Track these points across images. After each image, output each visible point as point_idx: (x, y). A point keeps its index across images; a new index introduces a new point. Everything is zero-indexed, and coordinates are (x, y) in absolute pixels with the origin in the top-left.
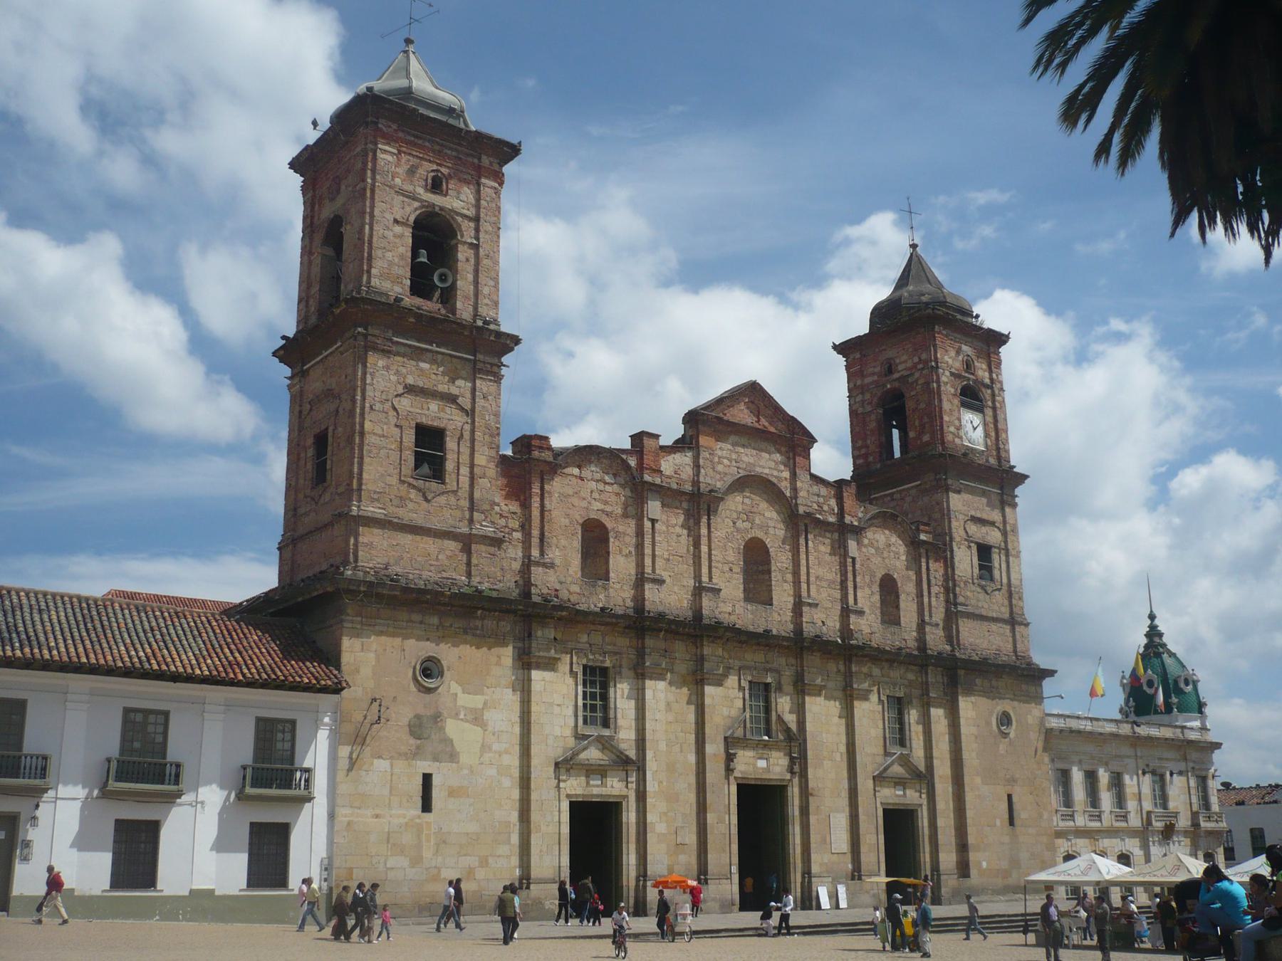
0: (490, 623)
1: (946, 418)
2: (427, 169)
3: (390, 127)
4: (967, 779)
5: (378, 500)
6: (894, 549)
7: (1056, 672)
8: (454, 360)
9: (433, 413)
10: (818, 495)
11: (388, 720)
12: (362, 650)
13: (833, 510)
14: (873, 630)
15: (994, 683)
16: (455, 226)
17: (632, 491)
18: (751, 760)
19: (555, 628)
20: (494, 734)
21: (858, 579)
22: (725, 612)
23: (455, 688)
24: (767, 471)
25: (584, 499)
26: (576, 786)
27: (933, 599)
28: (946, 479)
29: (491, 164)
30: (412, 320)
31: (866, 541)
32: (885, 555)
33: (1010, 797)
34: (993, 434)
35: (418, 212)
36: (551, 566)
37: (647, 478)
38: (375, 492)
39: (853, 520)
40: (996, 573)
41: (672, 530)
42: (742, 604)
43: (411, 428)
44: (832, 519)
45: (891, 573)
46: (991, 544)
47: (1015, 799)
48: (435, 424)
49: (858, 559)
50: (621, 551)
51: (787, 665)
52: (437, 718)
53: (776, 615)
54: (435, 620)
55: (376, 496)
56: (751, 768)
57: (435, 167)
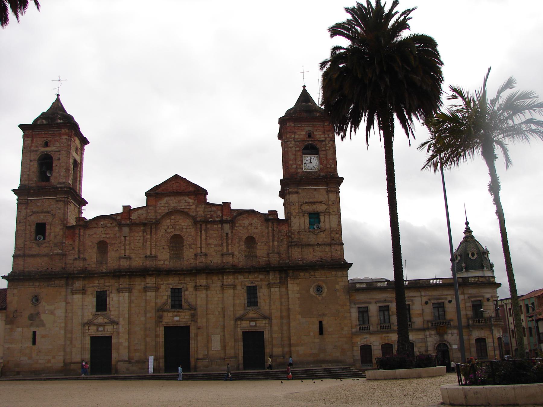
0: (57, 282)
1: (291, 162)
2: (40, 141)
4: (291, 317)
5: (21, 250)
6: (255, 225)
7: (352, 264)
8: (50, 200)
9: (41, 218)
10: (211, 211)
13: (219, 215)
14: (239, 260)
15: (312, 273)
16: (52, 156)
17: (118, 228)
18: (171, 318)
19: (83, 281)
20: (58, 317)
21: (230, 241)
22: (160, 265)
23: (44, 304)
24: (182, 208)
26: (92, 331)
27: (276, 243)
28: (289, 189)
29: (65, 131)
30: (32, 191)
31: (237, 225)
32: (249, 228)
33: (321, 323)
34: (325, 162)
36: (84, 259)
37: (123, 222)
39: (227, 217)
40: (322, 225)
42: (169, 260)
44: (217, 219)
45: (252, 235)
46: (319, 211)
47: (324, 323)
49: (230, 233)
50: (113, 250)
51: (191, 280)
52: (38, 314)
53: (185, 262)
54: (38, 284)
55: (21, 249)
56: (171, 321)
57: (45, 139)
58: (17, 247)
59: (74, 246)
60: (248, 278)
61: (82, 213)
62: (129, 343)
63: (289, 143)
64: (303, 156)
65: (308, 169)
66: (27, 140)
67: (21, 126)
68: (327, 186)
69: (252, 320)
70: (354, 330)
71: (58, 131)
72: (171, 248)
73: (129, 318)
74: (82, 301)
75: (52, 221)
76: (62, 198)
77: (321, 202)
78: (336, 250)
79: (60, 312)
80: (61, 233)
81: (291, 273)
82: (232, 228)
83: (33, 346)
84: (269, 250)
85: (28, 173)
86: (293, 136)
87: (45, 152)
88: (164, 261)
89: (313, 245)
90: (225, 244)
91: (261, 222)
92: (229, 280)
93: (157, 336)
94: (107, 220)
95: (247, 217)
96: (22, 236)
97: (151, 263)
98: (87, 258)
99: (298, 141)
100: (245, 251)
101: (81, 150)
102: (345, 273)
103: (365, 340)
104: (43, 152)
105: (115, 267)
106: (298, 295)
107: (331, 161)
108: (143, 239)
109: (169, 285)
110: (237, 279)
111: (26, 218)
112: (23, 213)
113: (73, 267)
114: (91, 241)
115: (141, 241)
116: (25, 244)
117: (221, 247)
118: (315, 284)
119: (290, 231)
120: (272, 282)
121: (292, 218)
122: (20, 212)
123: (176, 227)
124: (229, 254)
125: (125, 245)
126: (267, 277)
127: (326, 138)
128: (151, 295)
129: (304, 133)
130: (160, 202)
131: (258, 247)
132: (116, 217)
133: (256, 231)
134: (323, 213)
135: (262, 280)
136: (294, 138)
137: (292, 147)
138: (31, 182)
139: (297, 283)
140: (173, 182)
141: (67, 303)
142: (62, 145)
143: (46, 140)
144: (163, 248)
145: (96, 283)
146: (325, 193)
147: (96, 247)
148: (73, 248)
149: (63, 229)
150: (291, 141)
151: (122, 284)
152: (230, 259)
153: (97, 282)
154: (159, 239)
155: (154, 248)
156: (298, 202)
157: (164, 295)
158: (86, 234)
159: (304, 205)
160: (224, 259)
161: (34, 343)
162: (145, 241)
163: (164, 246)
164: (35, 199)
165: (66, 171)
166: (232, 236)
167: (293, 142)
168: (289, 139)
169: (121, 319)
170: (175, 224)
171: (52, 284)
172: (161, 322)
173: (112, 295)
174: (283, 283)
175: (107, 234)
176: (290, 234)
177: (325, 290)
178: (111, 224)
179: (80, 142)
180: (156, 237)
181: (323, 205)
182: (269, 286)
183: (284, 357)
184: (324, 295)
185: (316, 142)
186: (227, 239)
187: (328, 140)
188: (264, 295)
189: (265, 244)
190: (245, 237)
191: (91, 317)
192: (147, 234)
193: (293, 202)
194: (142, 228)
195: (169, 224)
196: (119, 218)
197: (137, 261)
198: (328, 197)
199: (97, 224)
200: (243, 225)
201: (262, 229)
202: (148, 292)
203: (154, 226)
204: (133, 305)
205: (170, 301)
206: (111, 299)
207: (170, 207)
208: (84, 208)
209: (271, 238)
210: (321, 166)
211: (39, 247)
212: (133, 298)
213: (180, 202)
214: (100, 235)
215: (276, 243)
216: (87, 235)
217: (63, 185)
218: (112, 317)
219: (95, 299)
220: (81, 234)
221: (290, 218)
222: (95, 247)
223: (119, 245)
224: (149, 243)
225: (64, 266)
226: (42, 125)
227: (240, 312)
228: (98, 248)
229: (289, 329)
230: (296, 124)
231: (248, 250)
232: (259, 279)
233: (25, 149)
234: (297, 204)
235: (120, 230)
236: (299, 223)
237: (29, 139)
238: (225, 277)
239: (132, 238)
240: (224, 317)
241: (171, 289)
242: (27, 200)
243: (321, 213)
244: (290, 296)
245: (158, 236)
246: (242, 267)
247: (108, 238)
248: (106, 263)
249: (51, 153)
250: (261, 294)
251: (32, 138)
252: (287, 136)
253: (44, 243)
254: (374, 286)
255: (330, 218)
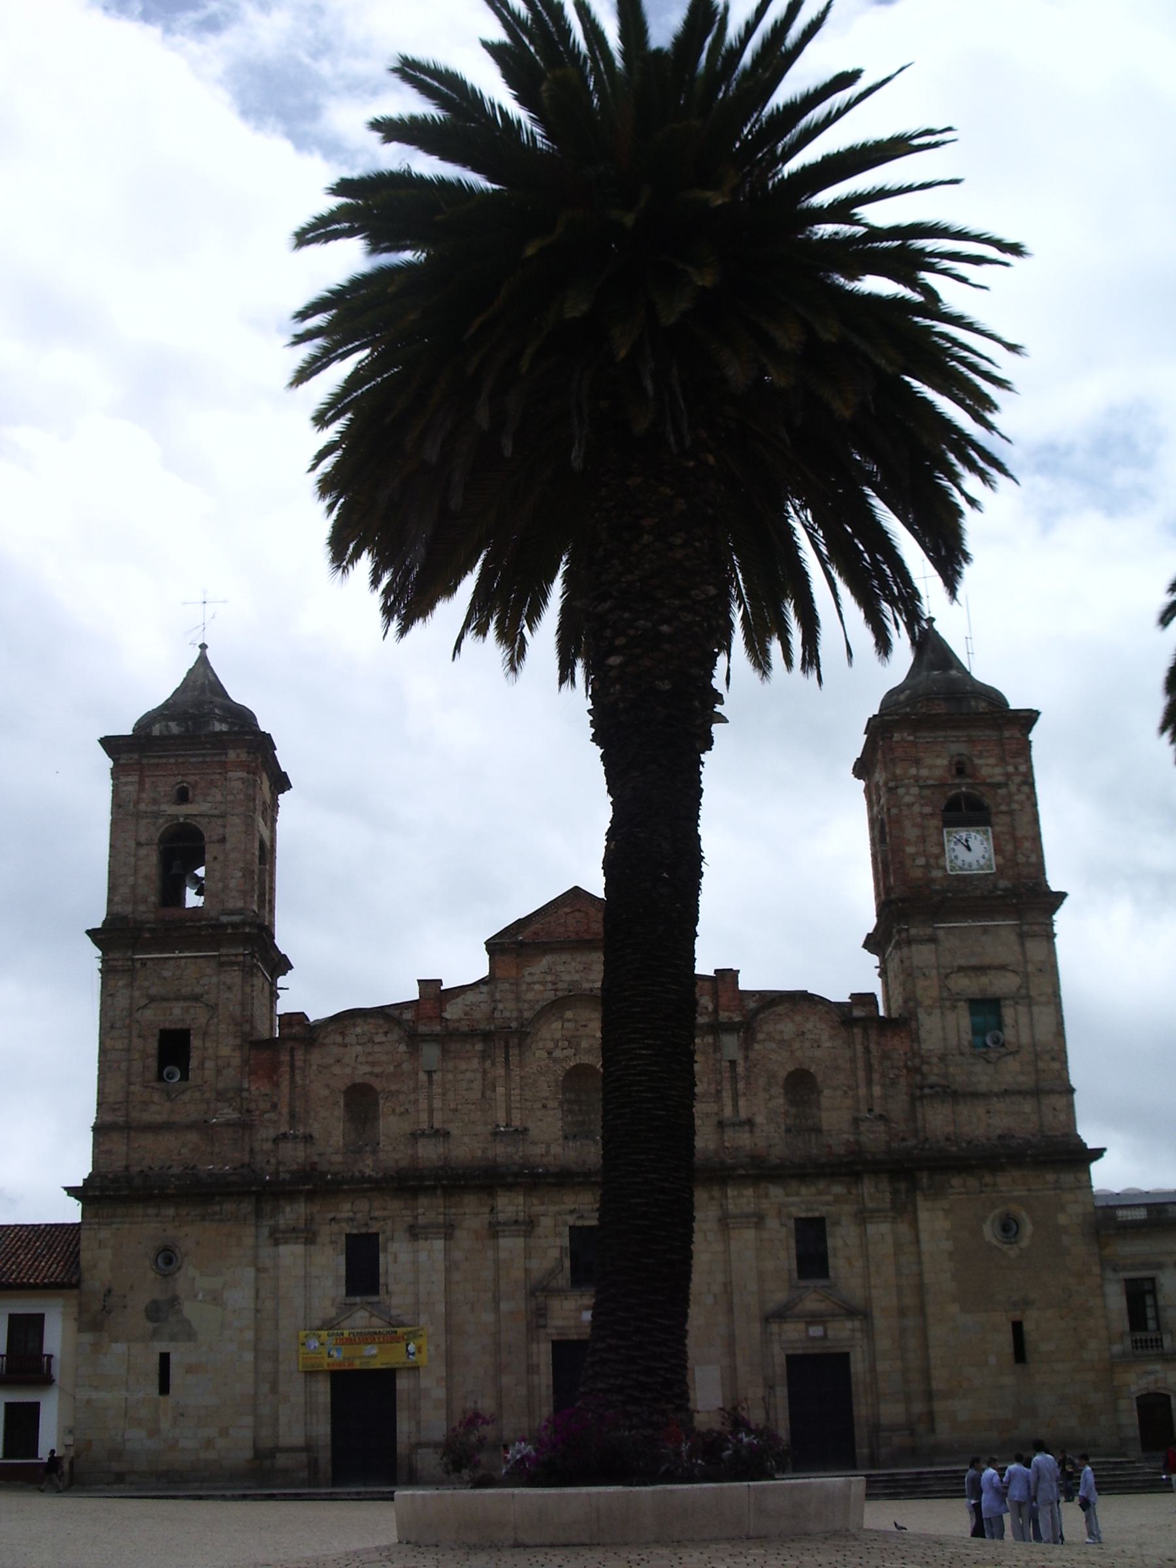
0: (229, 1207)
1: (910, 850)
2: (167, 785)
3: (131, 758)
5: (118, 1109)
6: (813, 1037)
8: (199, 961)
9: (176, 1015)
11: (125, 1307)
12: (100, 1247)
13: (707, 1008)
15: (988, 1179)
16: (201, 829)
17: (407, 1046)
21: (741, 1086)
25: (348, 1065)
27: (877, 1090)
28: (907, 930)
30: (147, 935)
31: (760, 1036)
32: (796, 1045)
33: (1017, 1327)
34: (1009, 847)
35: (163, 829)
36: (308, 1139)
37: (423, 1029)
38: (116, 1103)
39: (731, 1014)
40: (1009, 1034)
41: (460, 1076)
42: (561, 1141)
43: (154, 1035)
47: (1028, 1326)
48: (179, 1027)
50: (394, 1111)
52: (174, 1301)
54: (171, 1212)
55: (117, 1106)
57: (180, 778)
58: (106, 1100)
59: (275, 1099)
60: (798, 1194)
61: (278, 997)
62: (449, 1389)
63: (901, 791)
64: (945, 831)
65: (961, 869)
66: (126, 784)
67: (109, 743)
68: (1020, 919)
69: (814, 1318)
70: (1117, 1348)
71: (216, 754)
72: (565, 1108)
73: (448, 1315)
74: (305, 1266)
75: (207, 1024)
76: (236, 955)
77: (1003, 968)
78: (1054, 1109)
79: (240, 1298)
80: (236, 1061)
81: (924, 1179)
82: (747, 1044)
83: (161, 1398)
84: (858, 1110)
85: (131, 880)
86: (913, 771)
87: (181, 820)
88: (548, 1146)
89: (985, 1096)
90: (727, 1095)
91: (832, 1028)
92: (744, 1200)
93: (532, 1369)
94: (373, 1021)
95: (791, 1013)
96: (119, 1068)
97: (510, 1149)
98: (316, 1134)
99: (930, 786)
100: (786, 1113)
101: (273, 810)
102: (1083, 1177)
103: (1152, 1378)
104: (176, 817)
105: (404, 1163)
106: (948, 1245)
107: (1027, 845)
108: (484, 1080)
109: (564, 1217)
110: (767, 1196)
111: (130, 1015)
112: (122, 1001)
113: (273, 1161)
114: (328, 1086)
115: (477, 1085)
116: (128, 1093)
117: (714, 1102)
118: (997, 1211)
119: (915, 1054)
120: (870, 1205)
121: (921, 1014)
122: (111, 995)
123: (579, 1044)
124: (742, 1124)
125: (430, 1098)
126: (854, 1191)
127: (1008, 776)
128: (511, 1245)
129: (945, 762)
130: (529, 970)
131: (825, 1102)
132: (401, 1014)
133: (818, 1053)
134: (1013, 998)
135: (838, 1200)
136: (916, 778)
137: (913, 804)
138: (142, 908)
139: (944, 1210)
140: (567, 910)
141: (258, 1270)
142: (230, 798)
143: (182, 782)
144: (544, 1106)
145: (345, 1209)
146: (1013, 938)
147: (342, 1104)
148: (274, 1106)
149: (241, 1047)
150: (907, 787)
151: (424, 1214)
152: (744, 1139)
153: (348, 1206)
154: (531, 1081)
155: (518, 1105)
156: (938, 968)
157: (549, 1247)
158: (311, 1065)
159: (953, 976)
160: (726, 1138)
161: (164, 1388)
162: (489, 1086)
163: (546, 1099)
164: (156, 958)
165: (244, 875)
166: (747, 1069)
167: (915, 790)
168: (902, 780)
169: (424, 1319)
170: (578, 1033)
171: (215, 1213)
172: (545, 1327)
173: (394, 1247)
174: (903, 1209)
175: (373, 1064)
176: (917, 1062)
177: (1028, 1229)
178: (386, 1033)
179: (270, 786)
180: (523, 1074)
181: (1009, 974)
182: (863, 1217)
183: (912, 1433)
184: (1025, 1243)
185: (979, 788)
186: (734, 1079)
187: (1016, 781)
188: (846, 1245)
189: (845, 1092)
190: (786, 1073)
191: (332, 1312)
192: (493, 1064)
193: (922, 968)
194: (479, 1047)
195: (558, 1035)
196: (408, 1015)
197: (465, 1144)
198: (1024, 953)
199: (343, 1034)
200: (778, 1037)
201: (834, 1048)
202: (505, 1236)
203: (516, 1041)
204: (457, 1276)
205: (567, 1263)
206: (390, 1258)
207: (560, 983)
208: (281, 981)
209: (861, 1074)
210: (1001, 861)
211: (170, 1100)
212: (458, 1255)
213: (590, 969)
214: (354, 1068)
215: (877, 1090)
216: (314, 1067)
217: (236, 918)
218: (394, 1312)
219: (342, 1259)
220: (299, 1064)
221: (916, 1014)
222: (338, 1102)
223: (412, 1097)
224: (500, 1090)
225: (246, 1159)
226: (165, 741)
227: (779, 1296)
228: (347, 1105)
229: (925, 1347)
230: (919, 734)
231: (793, 1111)
232: (830, 1198)
233: (120, 810)
234: (934, 972)
235: (414, 1052)
236: (943, 1028)
237: (130, 779)
238: (730, 1192)
239: (450, 1076)
240: (730, 1310)
241: (570, 1227)
242: (133, 960)
243: (1006, 999)
244: (926, 1246)
245: (527, 1069)
246: (778, 1161)
247: (377, 1076)
248: (374, 1152)
249: (199, 823)
250: (839, 1243)
251: (140, 776)
252: (894, 772)
253: (184, 1092)
254: (1170, 1215)
255: (1031, 1013)
